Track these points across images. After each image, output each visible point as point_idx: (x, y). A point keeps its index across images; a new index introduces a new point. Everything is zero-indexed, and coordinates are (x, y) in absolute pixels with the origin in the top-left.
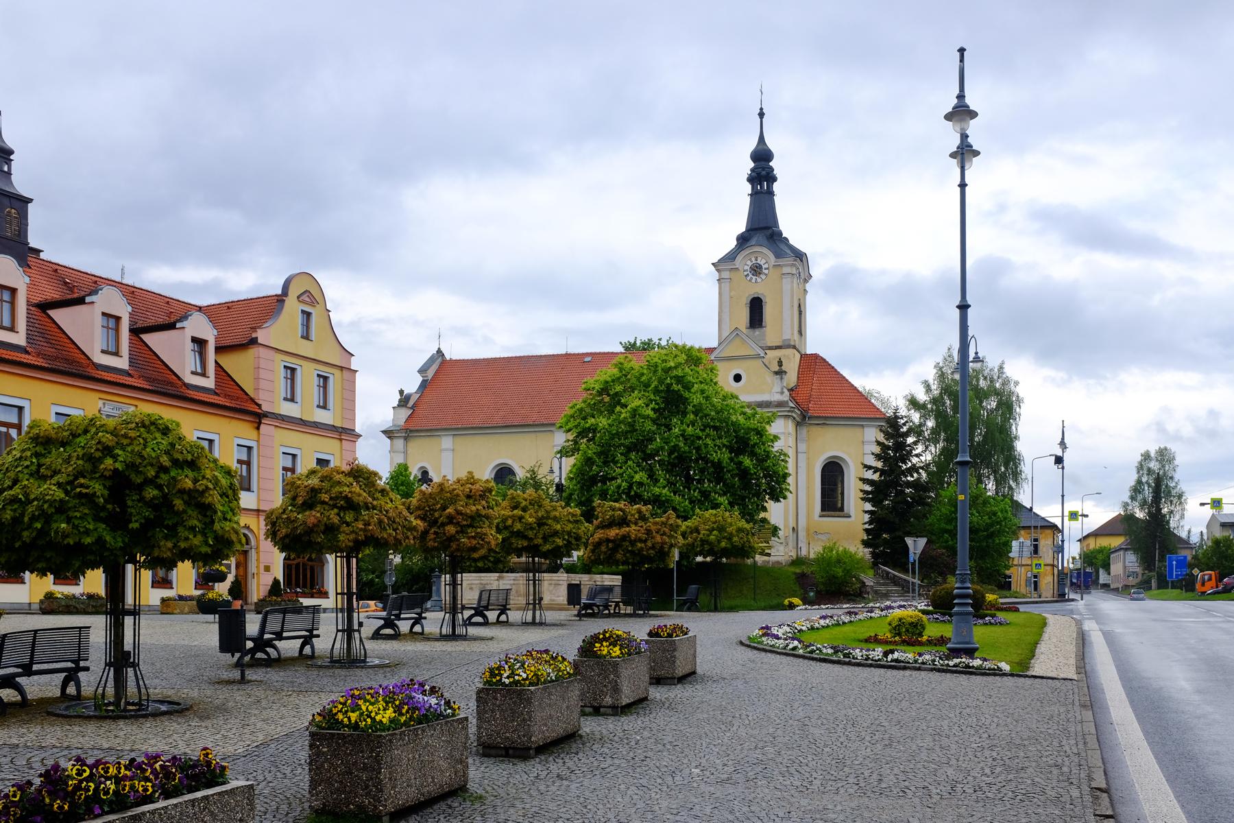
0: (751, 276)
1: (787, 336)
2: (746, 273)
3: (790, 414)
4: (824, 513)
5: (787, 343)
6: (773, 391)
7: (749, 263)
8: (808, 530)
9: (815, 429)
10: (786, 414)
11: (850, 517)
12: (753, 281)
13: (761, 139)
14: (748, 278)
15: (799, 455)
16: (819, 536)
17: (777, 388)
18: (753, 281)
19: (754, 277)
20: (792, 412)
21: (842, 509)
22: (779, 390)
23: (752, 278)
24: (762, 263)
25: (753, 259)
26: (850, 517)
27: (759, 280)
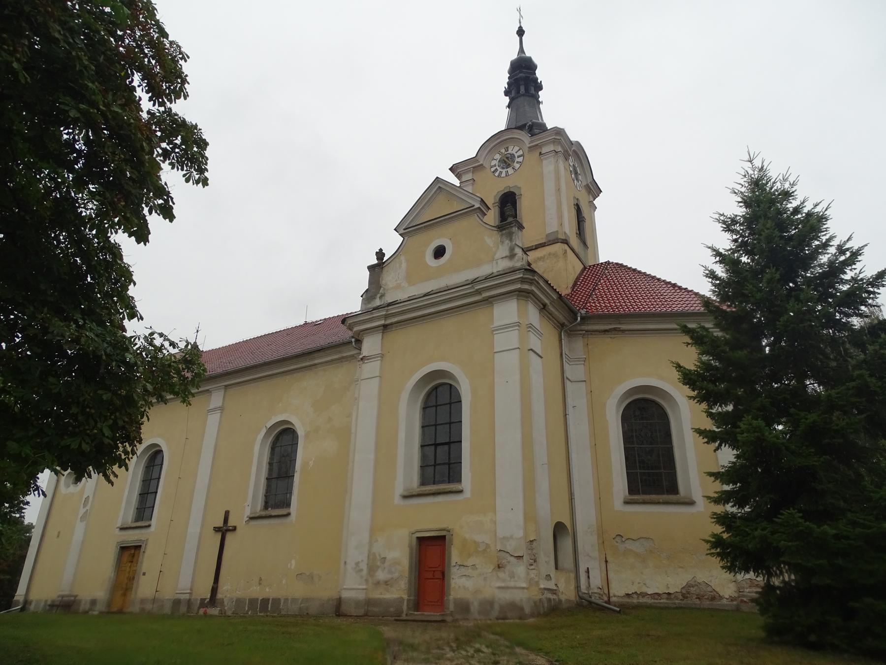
0: (499, 170)
1: (552, 227)
2: (493, 169)
3: (526, 287)
4: (636, 497)
5: (552, 238)
6: (497, 257)
7: (498, 157)
8: (601, 533)
9: (601, 344)
10: (518, 286)
11: (691, 503)
12: (503, 175)
13: (521, 50)
14: (497, 174)
15: (568, 383)
16: (629, 545)
17: (504, 251)
18: (503, 175)
19: (504, 171)
20: (531, 282)
21: (673, 489)
22: (507, 253)
23: (501, 172)
24: (514, 152)
25: (503, 151)
26: (691, 503)
27: (510, 171)
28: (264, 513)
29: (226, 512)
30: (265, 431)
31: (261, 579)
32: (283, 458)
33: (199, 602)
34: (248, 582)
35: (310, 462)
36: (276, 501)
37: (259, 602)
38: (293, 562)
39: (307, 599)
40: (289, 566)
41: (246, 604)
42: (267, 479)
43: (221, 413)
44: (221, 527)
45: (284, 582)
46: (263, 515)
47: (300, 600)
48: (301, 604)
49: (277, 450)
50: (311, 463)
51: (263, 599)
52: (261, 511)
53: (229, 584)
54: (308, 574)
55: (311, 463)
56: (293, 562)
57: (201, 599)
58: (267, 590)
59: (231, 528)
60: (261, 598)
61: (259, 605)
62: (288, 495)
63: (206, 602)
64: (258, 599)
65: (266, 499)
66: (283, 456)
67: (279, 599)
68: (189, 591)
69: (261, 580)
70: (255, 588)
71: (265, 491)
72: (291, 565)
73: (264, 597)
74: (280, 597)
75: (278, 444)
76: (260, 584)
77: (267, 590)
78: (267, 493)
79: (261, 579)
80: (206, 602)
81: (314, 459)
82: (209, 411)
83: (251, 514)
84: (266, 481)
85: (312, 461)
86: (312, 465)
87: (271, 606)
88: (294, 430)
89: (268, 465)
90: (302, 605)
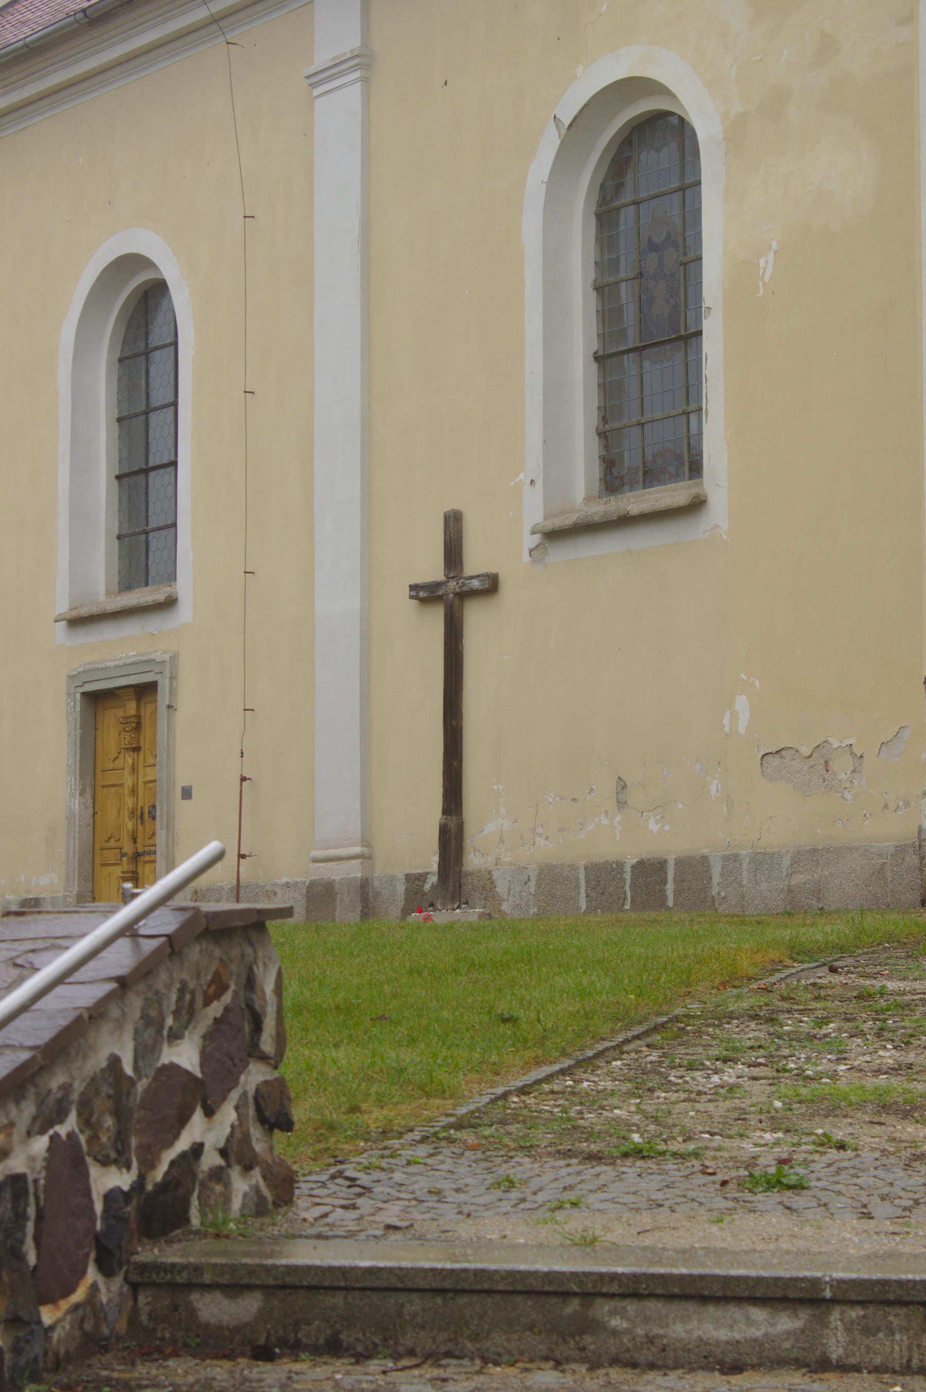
28: (600, 509)
29: (447, 518)
30: (558, 142)
31: (622, 786)
32: (653, 256)
33: (401, 888)
34: (574, 800)
35: (762, 262)
36: (649, 457)
37: (628, 876)
38: (742, 703)
39: (815, 851)
40: (726, 722)
41: (577, 887)
42: (599, 359)
43: (365, 80)
44: (438, 585)
45: (714, 788)
46: (597, 518)
47: (786, 862)
48: (790, 875)
49: (627, 217)
50: (767, 264)
51: (641, 863)
52: (588, 499)
53: (503, 811)
54: (806, 751)
55: (767, 264)
56: (742, 703)
57: (409, 878)
58: (653, 826)
59: (476, 584)
60: (631, 861)
61: (627, 888)
62: (693, 418)
63: (427, 887)
64: (620, 865)
65: (606, 447)
66: (653, 247)
67: (704, 860)
68: (357, 850)
69: (624, 787)
70: (605, 821)
71: (595, 415)
72: (734, 715)
73: (644, 856)
74: (706, 851)
75: (627, 196)
76: (622, 804)
77: (653, 826)
78: (604, 420)
79: (622, 786)
80: (427, 887)
81: (774, 245)
82: (316, 79)
83: (545, 518)
84: (594, 367)
85: (771, 257)
86: (770, 270)
87: (678, 892)
88: (682, 120)
89: (593, 295)
90: (797, 879)
